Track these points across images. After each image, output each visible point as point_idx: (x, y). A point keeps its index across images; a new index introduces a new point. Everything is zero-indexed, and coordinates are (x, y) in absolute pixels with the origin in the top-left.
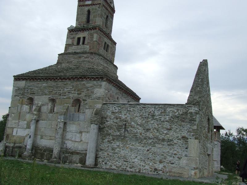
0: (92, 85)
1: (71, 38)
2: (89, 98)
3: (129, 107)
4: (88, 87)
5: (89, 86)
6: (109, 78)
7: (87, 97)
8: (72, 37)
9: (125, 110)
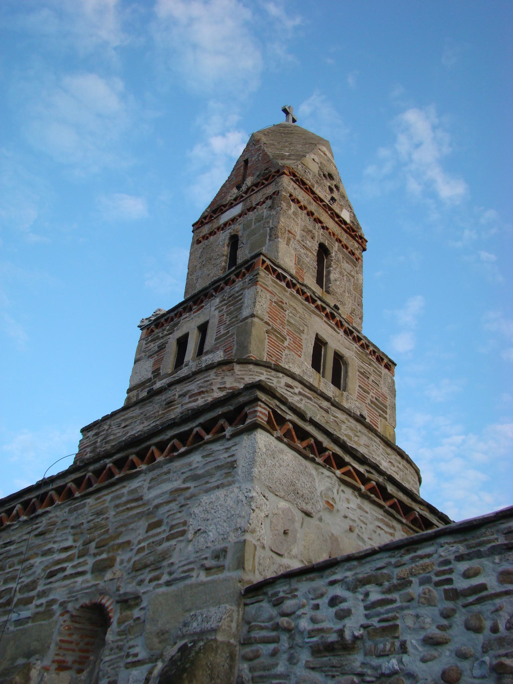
0: (178, 484)
1: (149, 357)
2: (157, 578)
3: (460, 558)
4: (157, 507)
5: (156, 502)
6: (290, 416)
7: (147, 575)
8: (156, 347)
9: (430, 602)
